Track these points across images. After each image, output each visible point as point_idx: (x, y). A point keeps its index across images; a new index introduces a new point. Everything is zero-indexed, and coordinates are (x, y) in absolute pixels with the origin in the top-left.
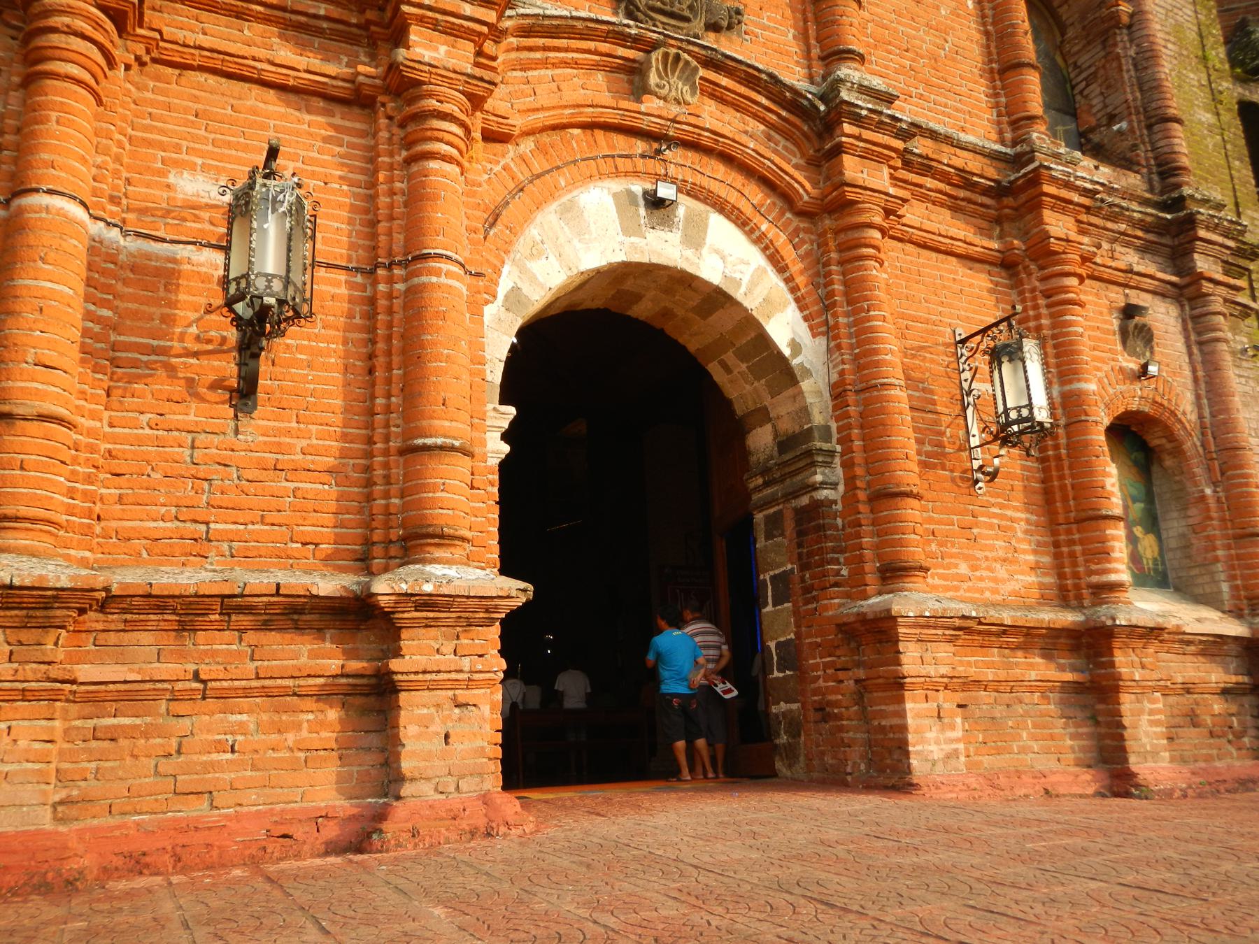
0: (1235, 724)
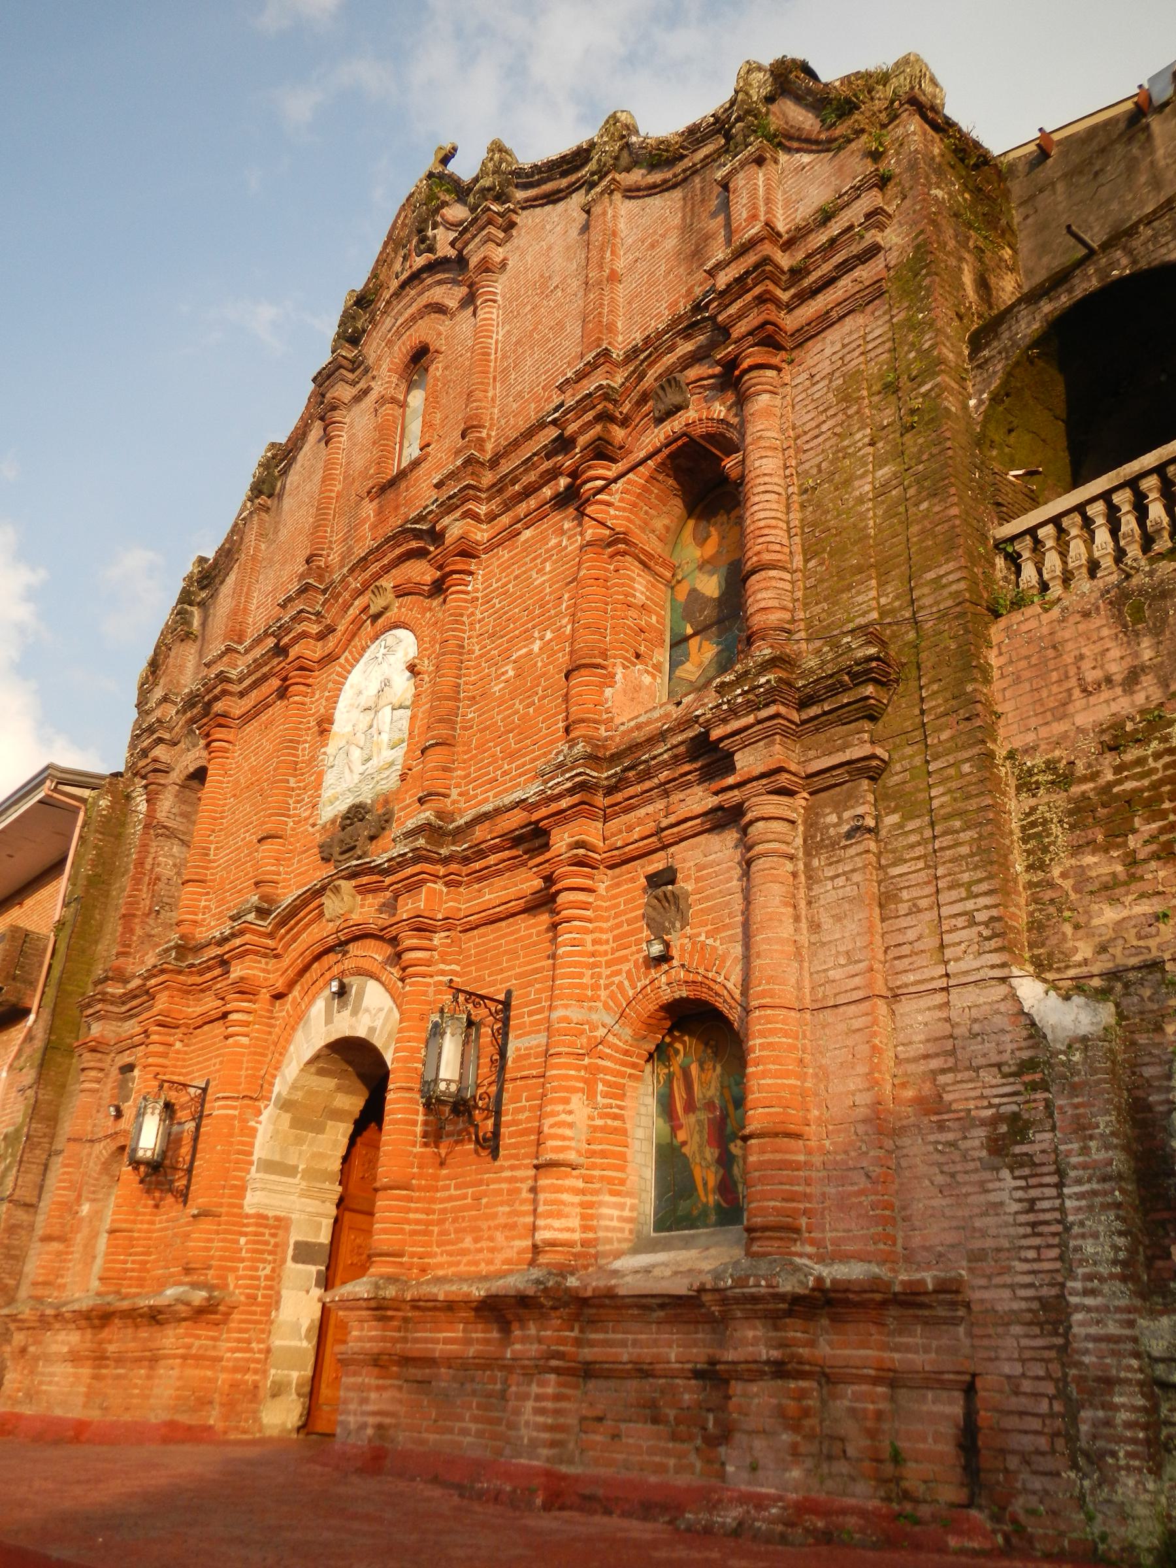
0: (710, 1425)
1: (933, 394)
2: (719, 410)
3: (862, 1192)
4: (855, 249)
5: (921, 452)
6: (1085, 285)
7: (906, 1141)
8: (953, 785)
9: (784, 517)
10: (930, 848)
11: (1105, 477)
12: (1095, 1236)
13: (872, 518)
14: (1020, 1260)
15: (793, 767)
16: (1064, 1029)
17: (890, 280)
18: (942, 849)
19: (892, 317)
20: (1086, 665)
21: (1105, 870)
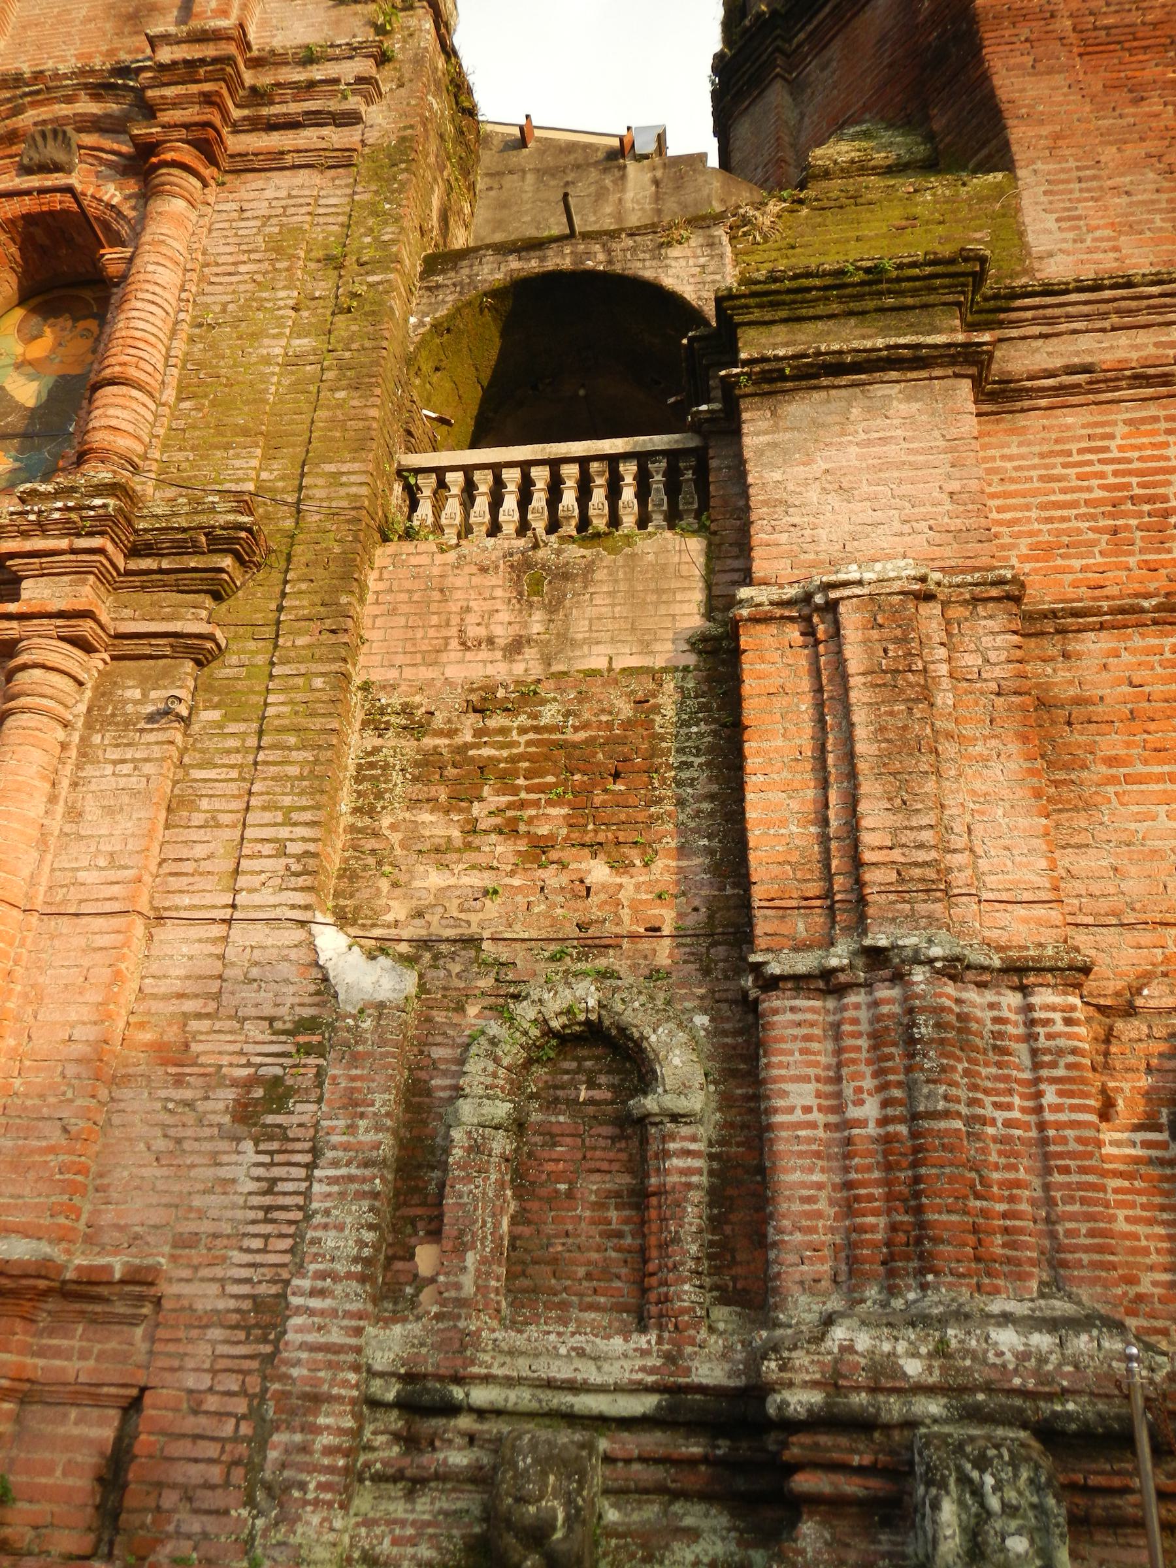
1: (381, 288)
2: (112, 193)
3: (51, 1150)
4: (334, 105)
5: (351, 339)
6: (558, 261)
7: (126, 1093)
8: (299, 697)
9: (166, 341)
10: (250, 758)
11: (529, 447)
12: (340, 1228)
13: (275, 384)
14: (241, 1249)
15: (104, 618)
16: (360, 990)
17: (363, 156)
18: (266, 763)
19: (354, 193)
20: (471, 619)
21: (440, 831)
